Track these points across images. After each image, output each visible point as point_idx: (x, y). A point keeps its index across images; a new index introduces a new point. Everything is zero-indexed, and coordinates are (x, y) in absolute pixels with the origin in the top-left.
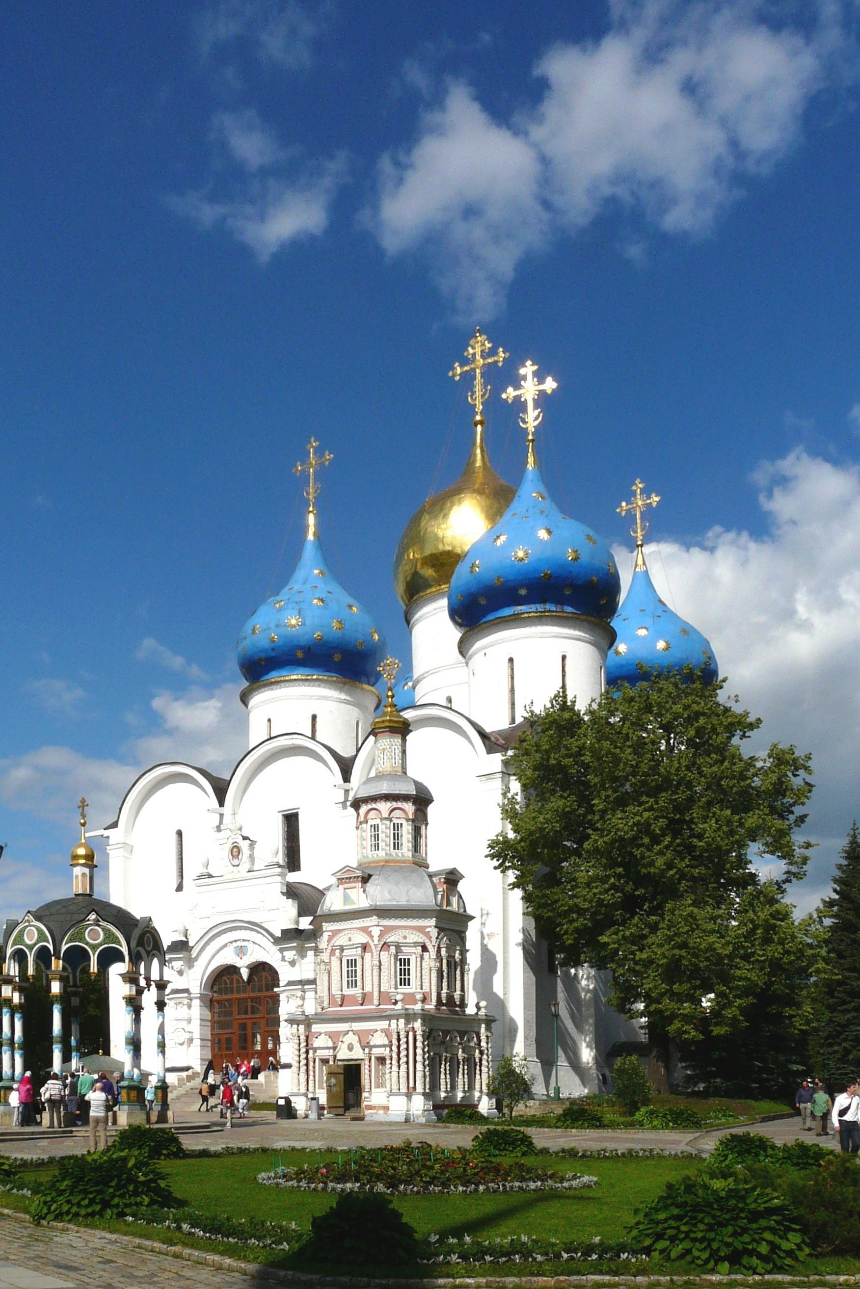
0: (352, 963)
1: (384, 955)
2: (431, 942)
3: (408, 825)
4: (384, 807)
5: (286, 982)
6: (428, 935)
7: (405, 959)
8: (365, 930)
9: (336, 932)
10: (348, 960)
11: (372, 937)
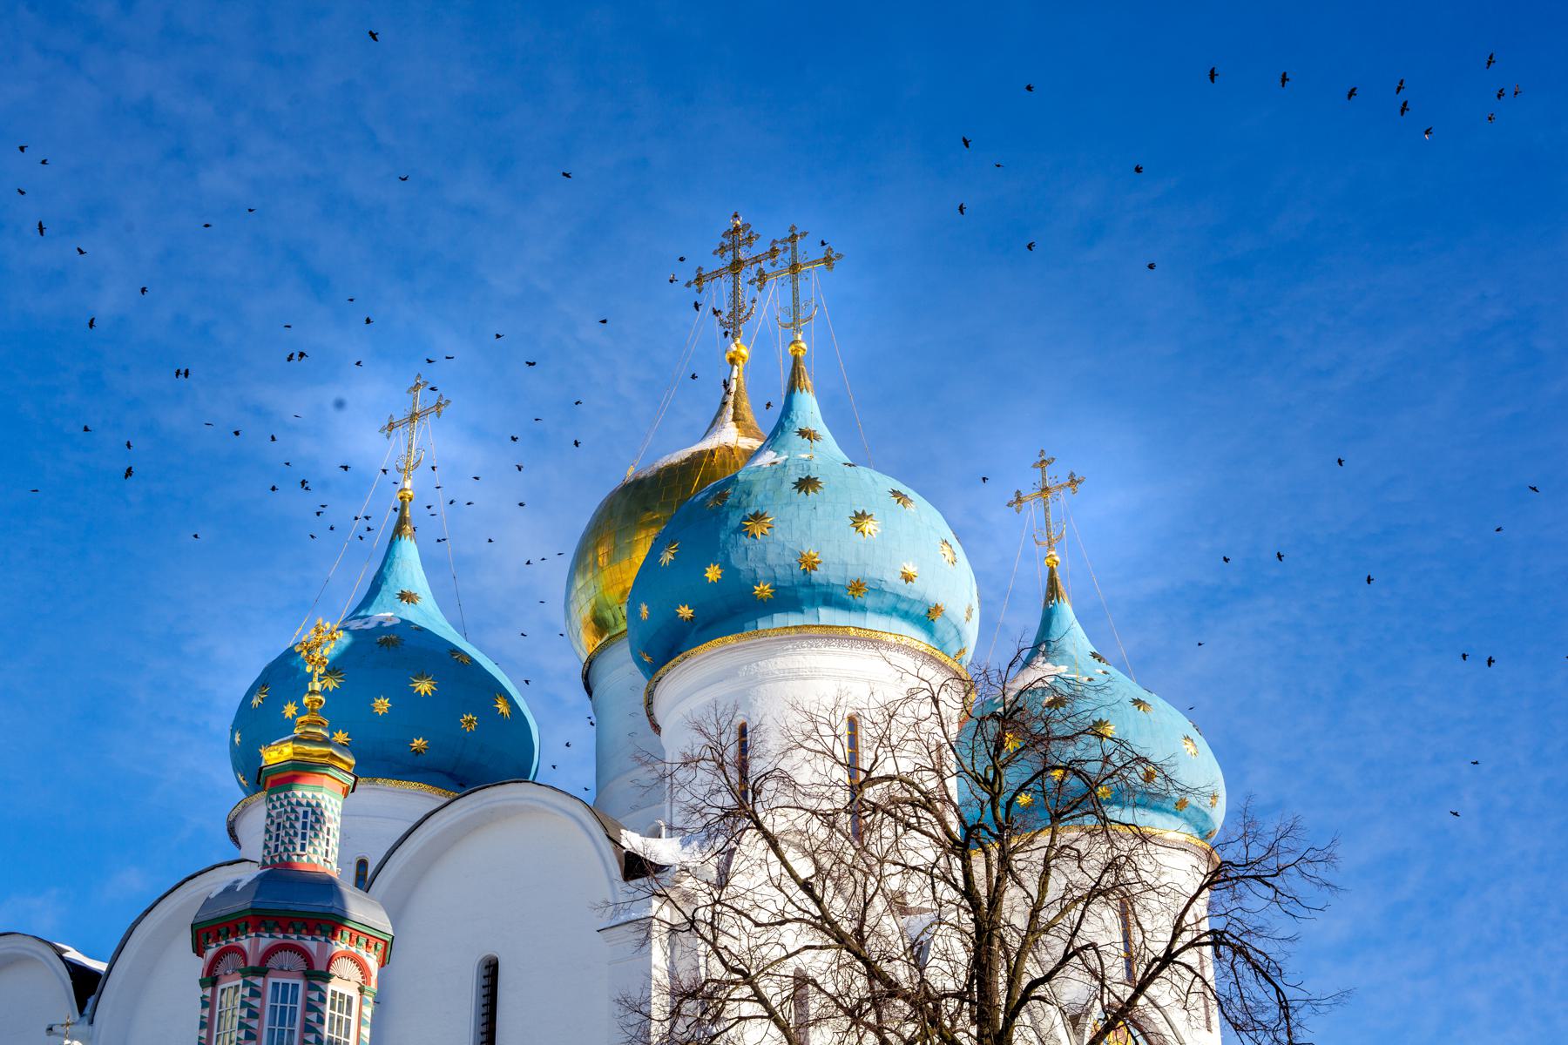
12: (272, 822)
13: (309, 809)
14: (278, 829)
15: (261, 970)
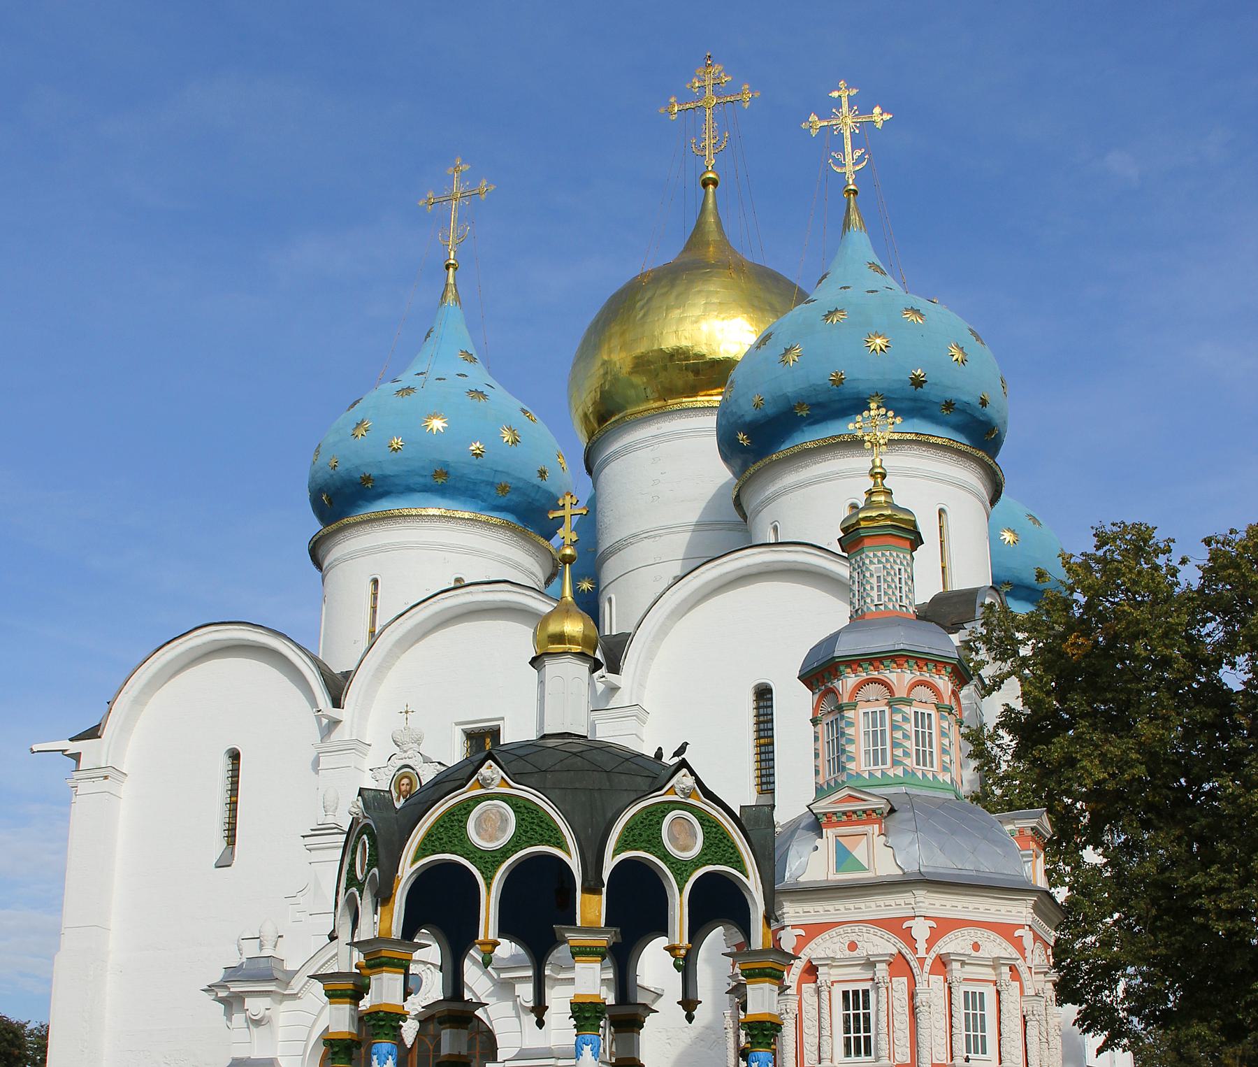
0: (857, 1000)
1: (937, 981)
2: (1025, 958)
3: (942, 717)
4: (901, 678)
5: (513, 1052)
6: (1018, 943)
7: (974, 993)
8: (896, 926)
9: (813, 931)
10: (846, 994)
11: (911, 941)
12: (872, 575)
13: (902, 568)
14: (879, 581)
15: (908, 702)
